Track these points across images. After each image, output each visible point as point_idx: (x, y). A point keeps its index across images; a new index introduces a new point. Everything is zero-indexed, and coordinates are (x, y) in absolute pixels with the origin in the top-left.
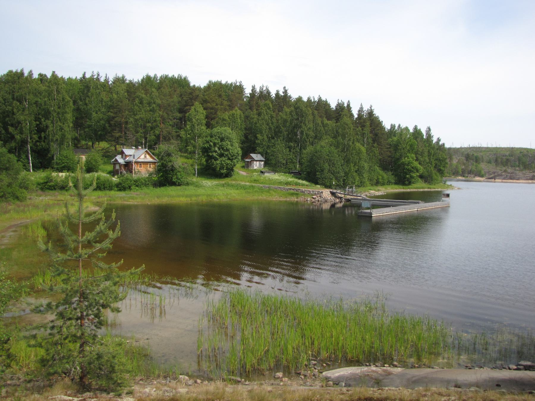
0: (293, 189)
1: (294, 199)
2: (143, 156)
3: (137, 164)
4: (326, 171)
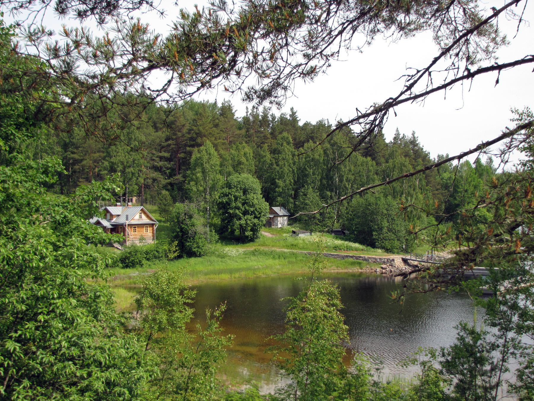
0: (352, 257)
1: (356, 270)
2: (137, 217)
3: (131, 227)
4: (385, 230)
